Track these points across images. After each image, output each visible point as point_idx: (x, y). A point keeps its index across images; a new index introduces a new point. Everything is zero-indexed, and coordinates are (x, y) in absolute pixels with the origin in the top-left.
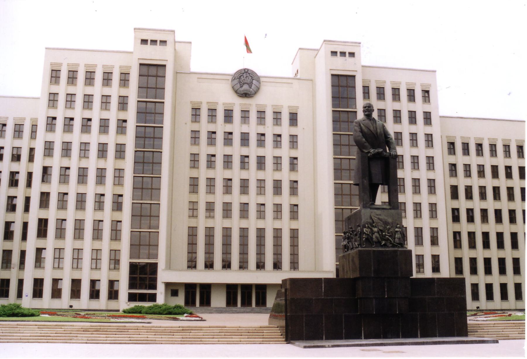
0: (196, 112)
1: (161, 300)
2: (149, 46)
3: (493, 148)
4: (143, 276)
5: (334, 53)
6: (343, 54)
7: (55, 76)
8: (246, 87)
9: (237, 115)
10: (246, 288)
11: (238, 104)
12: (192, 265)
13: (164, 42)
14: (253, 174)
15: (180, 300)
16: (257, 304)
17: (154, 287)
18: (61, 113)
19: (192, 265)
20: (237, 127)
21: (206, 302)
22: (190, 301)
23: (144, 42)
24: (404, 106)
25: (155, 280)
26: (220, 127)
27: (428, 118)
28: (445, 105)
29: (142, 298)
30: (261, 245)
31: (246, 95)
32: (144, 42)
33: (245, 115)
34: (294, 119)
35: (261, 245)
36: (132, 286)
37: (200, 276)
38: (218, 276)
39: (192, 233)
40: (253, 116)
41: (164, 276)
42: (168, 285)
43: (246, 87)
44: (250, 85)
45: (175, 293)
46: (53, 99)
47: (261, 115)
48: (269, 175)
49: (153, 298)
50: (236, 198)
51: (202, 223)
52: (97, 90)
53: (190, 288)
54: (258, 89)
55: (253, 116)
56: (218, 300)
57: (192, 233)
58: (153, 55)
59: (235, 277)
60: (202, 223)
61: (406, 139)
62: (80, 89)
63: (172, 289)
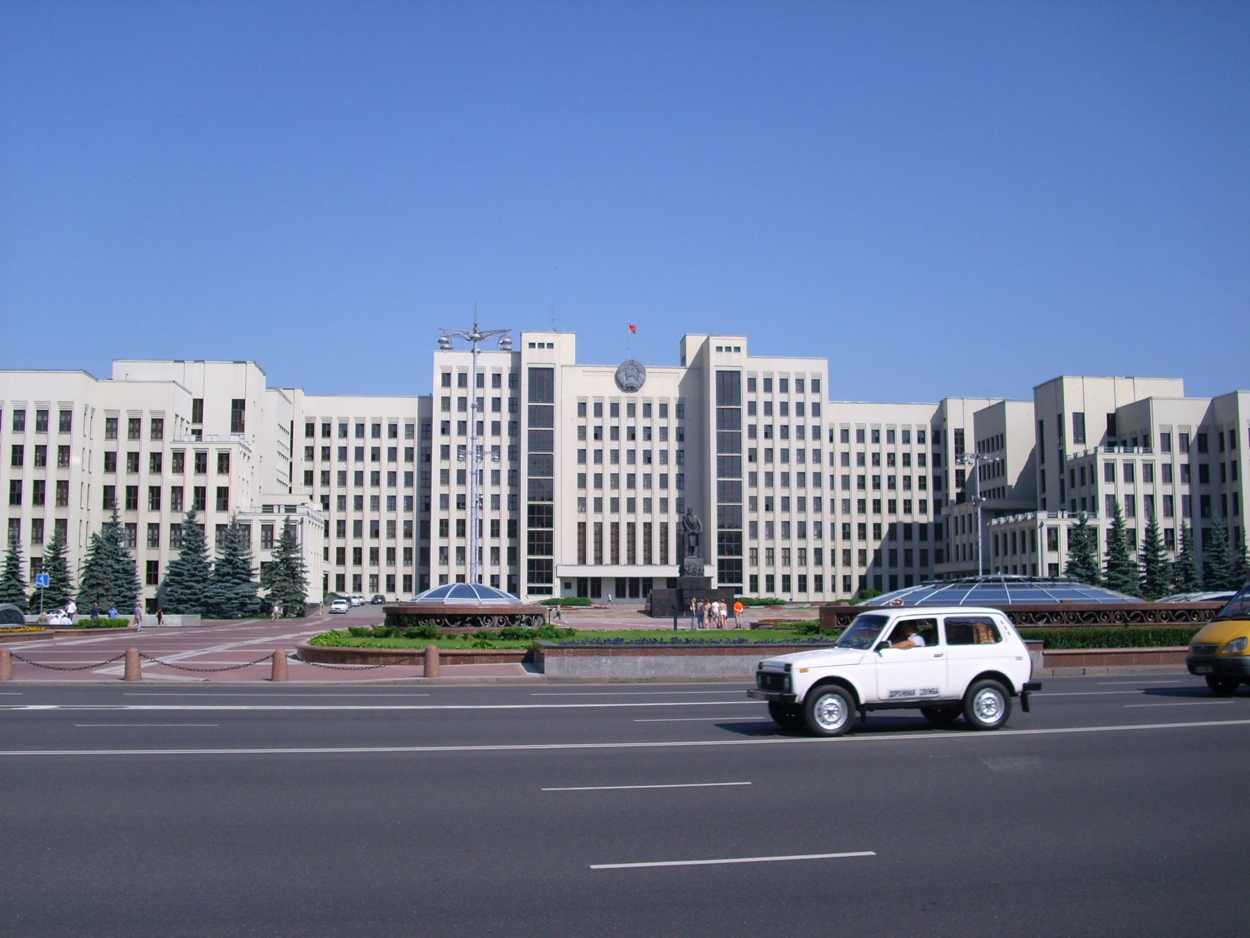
0: (582, 408)
1: (557, 593)
3: (891, 434)
8: (632, 380)
9: (623, 410)
10: (634, 581)
11: (624, 398)
14: (641, 469)
15: (573, 593)
17: (550, 580)
19: (582, 560)
20: (624, 422)
21: (597, 593)
22: (582, 592)
26: (607, 422)
29: (540, 591)
31: (632, 389)
33: (632, 409)
36: (530, 579)
37: (590, 571)
38: (608, 571)
39: (582, 526)
40: (640, 410)
42: (562, 578)
47: (648, 408)
49: (549, 591)
50: (624, 493)
51: (591, 518)
55: (640, 410)
59: (625, 571)
60: (591, 518)
63: (567, 583)
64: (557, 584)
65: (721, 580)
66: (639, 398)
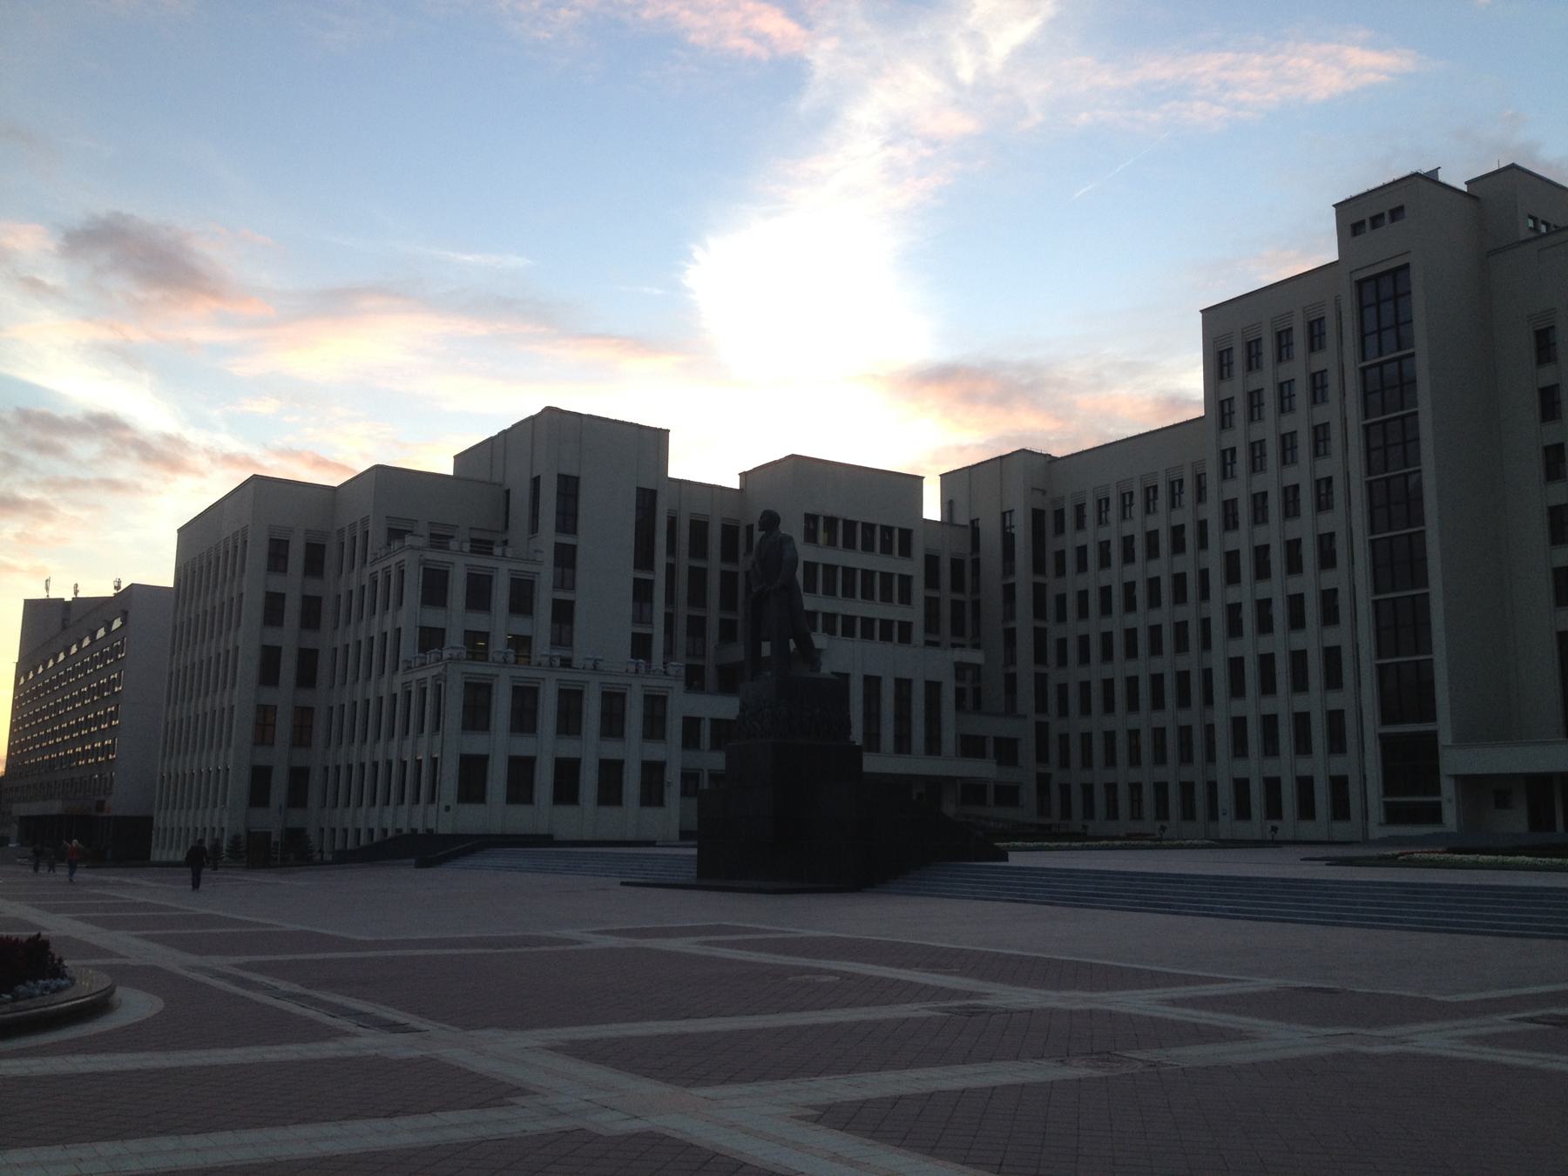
4: (1411, 765)
7: (1218, 363)
18: (1237, 438)
25: (1435, 770)
36: (1389, 787)
41: (1455, 761)
49: (1433, 814)
58: (1382, 249)
64: (1448, 789)
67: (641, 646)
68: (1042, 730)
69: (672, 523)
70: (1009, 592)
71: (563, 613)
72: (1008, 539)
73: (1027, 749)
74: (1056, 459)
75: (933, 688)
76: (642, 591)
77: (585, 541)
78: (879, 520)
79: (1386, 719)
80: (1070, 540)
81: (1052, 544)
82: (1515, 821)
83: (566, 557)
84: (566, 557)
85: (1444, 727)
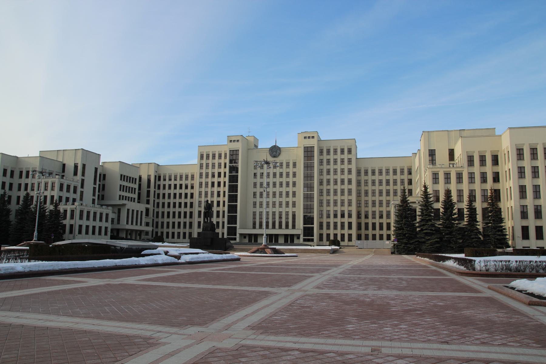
1: (238, 240)
2: (233, 143)
5: (305, 138)
6: (309, 137)
7: (202, 157)
12: (254, 227)
13: (238, 141)
16: (290, 242)
17: (236, 235)
18: (204, 171)
22: (250, 241)
23: (231, 141)
24: (339, 157)
27: (350, 161)
28: (363, 152)
30: (280, 218)
31: (274, 157)
32: (231, 141)
34: (295, 165)
35: (280, 218)
39: (254, 214)
41: (239, 231)
42: (241, 234)
43: (275, 153)
44: (276, 152)
45: (245, 237)
46: (201, 166)
47: (281, 165)
48: (284, 189)
49: (235, 239)
52: (216, 161)
53: (250, 235)
54: (280, 154)
56: (281, 240)
57: (254, 214)
58: (234, 146)
61: (215, 204)
62: (210, 161)
63: (243, 236)
64: (238, 235)
65: (228, 235)
66: (278, 160)
67: (94, 200)
68: (153, 220)
69: (100, 175)
70: (148, 192)
71: (82, 193)
72: (149, 181)
73: (151, 224)
74: (158, 165)
75: (142, 212)
76: (94, 188)
77: (86, 178)
78: (129, 175)
79: (228, 224)
80: (162, 183)
81: (158, 183)
82: (246, 240)
83: (83, 181)
84: (83, 181)
85: (238, 226)
